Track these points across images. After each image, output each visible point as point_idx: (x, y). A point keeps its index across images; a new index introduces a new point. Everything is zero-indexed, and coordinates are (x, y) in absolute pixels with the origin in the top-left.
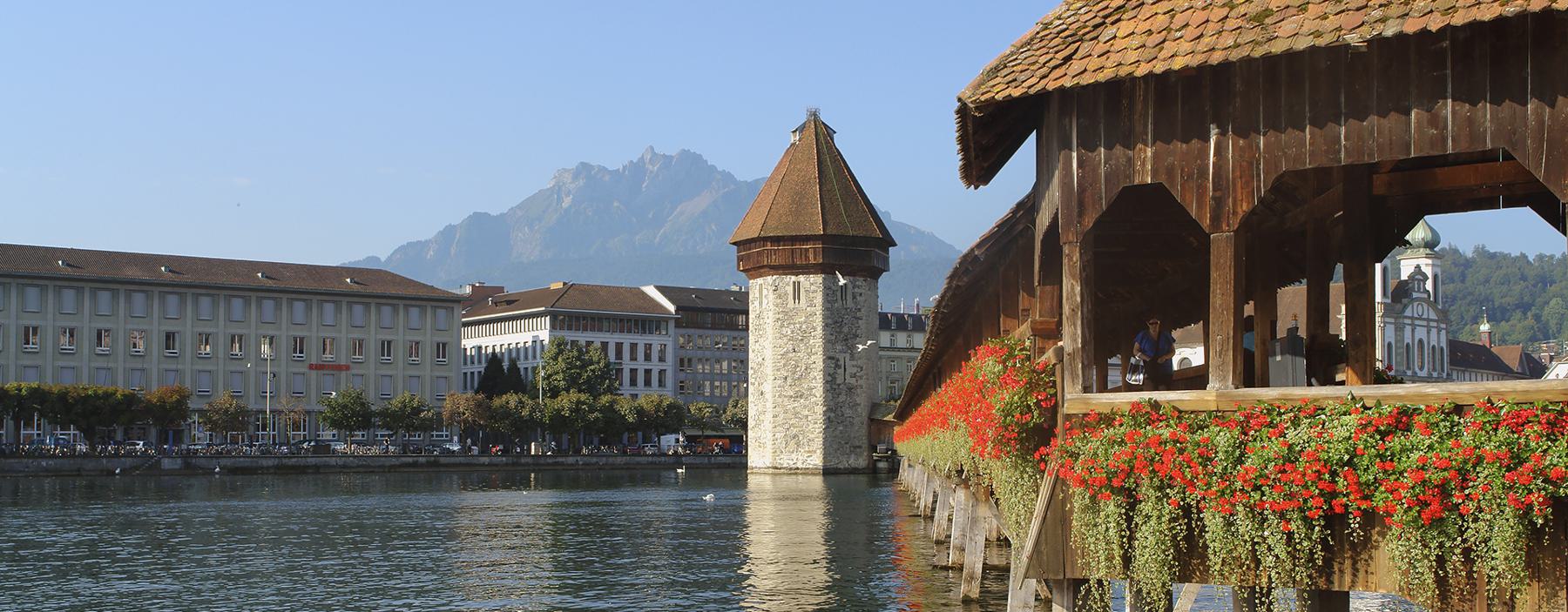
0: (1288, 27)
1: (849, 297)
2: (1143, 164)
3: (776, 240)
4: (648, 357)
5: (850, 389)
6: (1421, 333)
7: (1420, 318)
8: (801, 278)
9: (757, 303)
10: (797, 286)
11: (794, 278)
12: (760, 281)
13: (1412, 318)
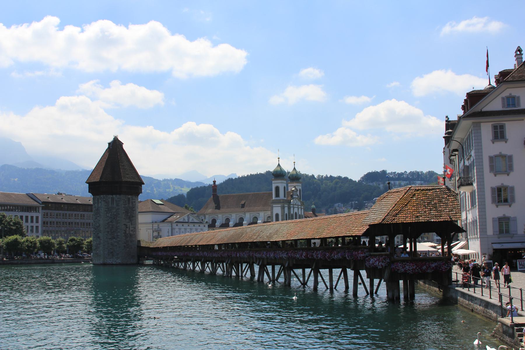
1: (131, 204)
4: (32, 221)
5: (131, 235)
6: (296, 210)
7: (296, 205)
8: (114, 196)
10: (113, 199)
12: (97, 197)
13: (293, 205)
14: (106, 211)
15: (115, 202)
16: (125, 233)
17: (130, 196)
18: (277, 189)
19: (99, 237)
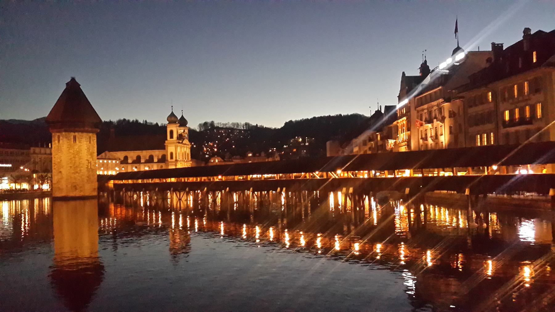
8: (76, 134)
9: (57, 142)
15: (77, 139)
16: (87, 168)
18: (172, 132)
19: (60, 172)
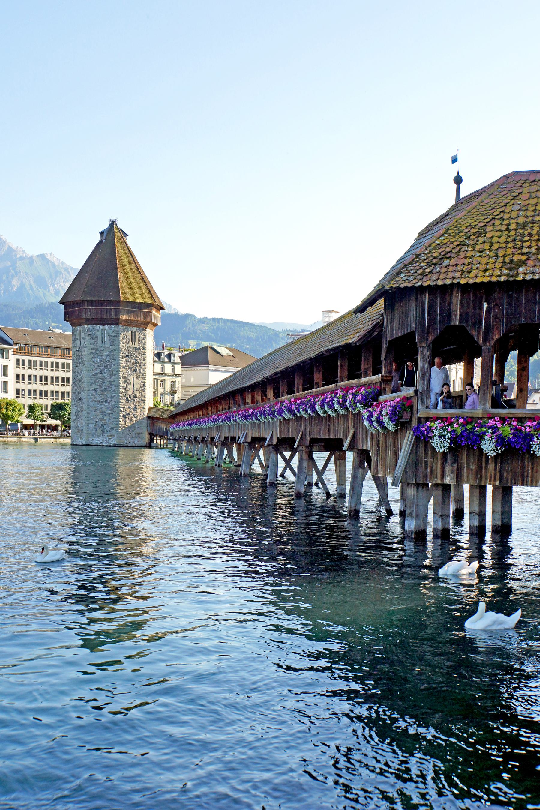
0: (521, 269)
2: (456, 316)
3: (91, 303)
8: (107, 327)
10: (103, 332)
11: (101, 327)
12: (79, 328)
14: (92, 353)
17: (135, 329)
19: (80, 399)
